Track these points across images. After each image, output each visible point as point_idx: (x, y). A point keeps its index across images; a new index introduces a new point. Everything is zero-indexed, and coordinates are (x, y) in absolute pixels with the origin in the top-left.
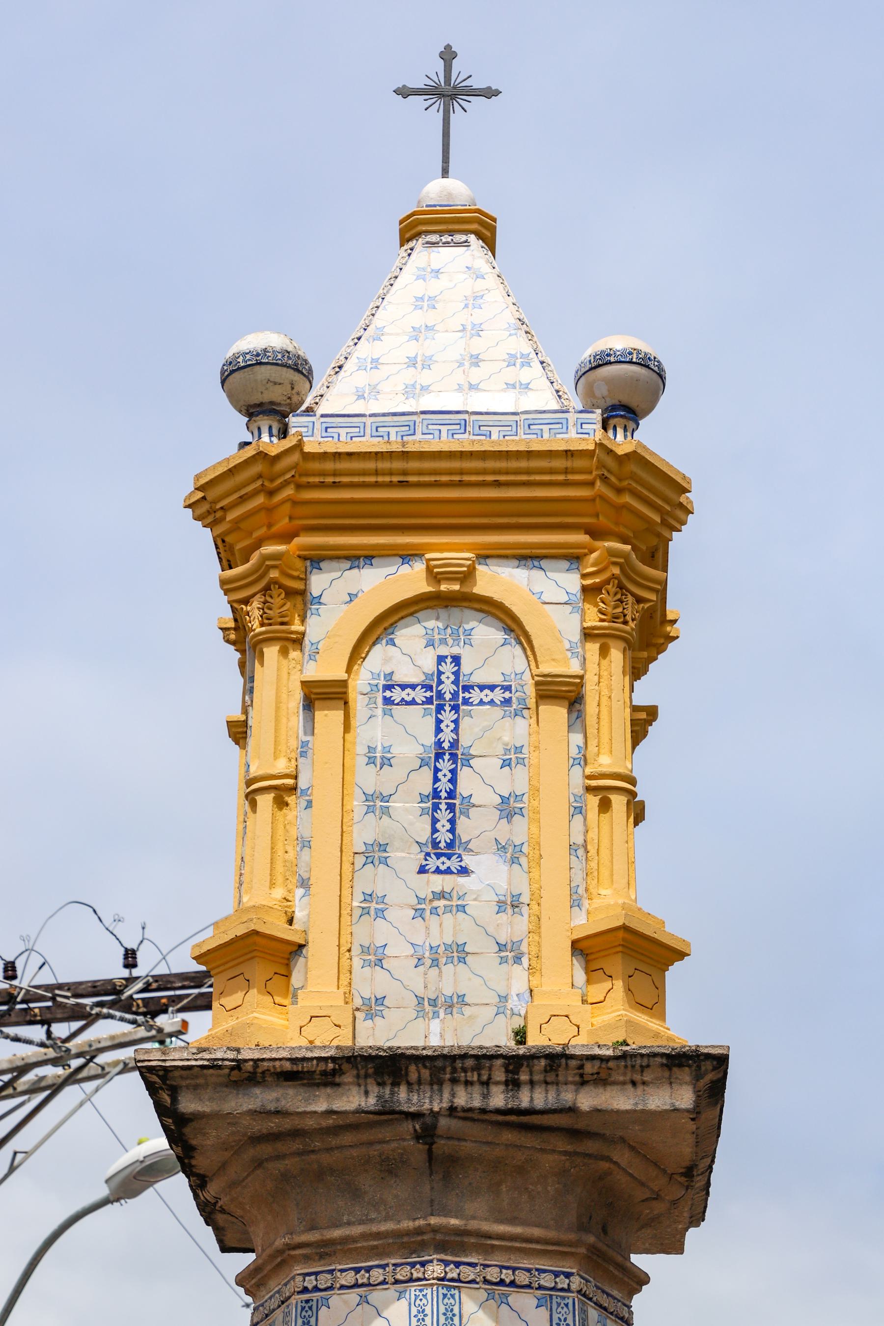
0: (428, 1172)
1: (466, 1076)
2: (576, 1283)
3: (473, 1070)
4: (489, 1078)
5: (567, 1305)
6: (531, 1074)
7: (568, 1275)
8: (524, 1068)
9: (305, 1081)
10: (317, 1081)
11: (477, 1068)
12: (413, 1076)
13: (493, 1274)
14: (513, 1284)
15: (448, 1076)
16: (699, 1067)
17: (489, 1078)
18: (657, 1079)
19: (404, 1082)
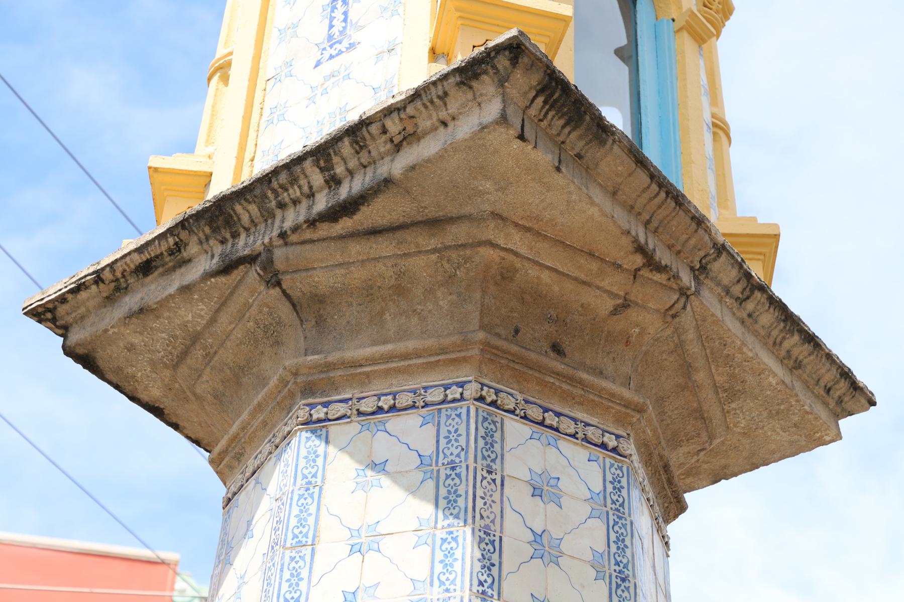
0: (298, 322)
1: (289, 195)
2: (471, 390)
3: (292, 184)
4: (311, 188)
5: (459, 416)
6: (344, 160)
7: (461, 385)
8: (336, 159)
9: (161, 270)
10: (171, 264)
11: (294, 181)
12: (245, 219)
13: (367, 406)
14: (393, 408)
15: (274, 203)
16: (494, 67)
17: (311, 188)
18: (463, 105)
19: (242, 230)
